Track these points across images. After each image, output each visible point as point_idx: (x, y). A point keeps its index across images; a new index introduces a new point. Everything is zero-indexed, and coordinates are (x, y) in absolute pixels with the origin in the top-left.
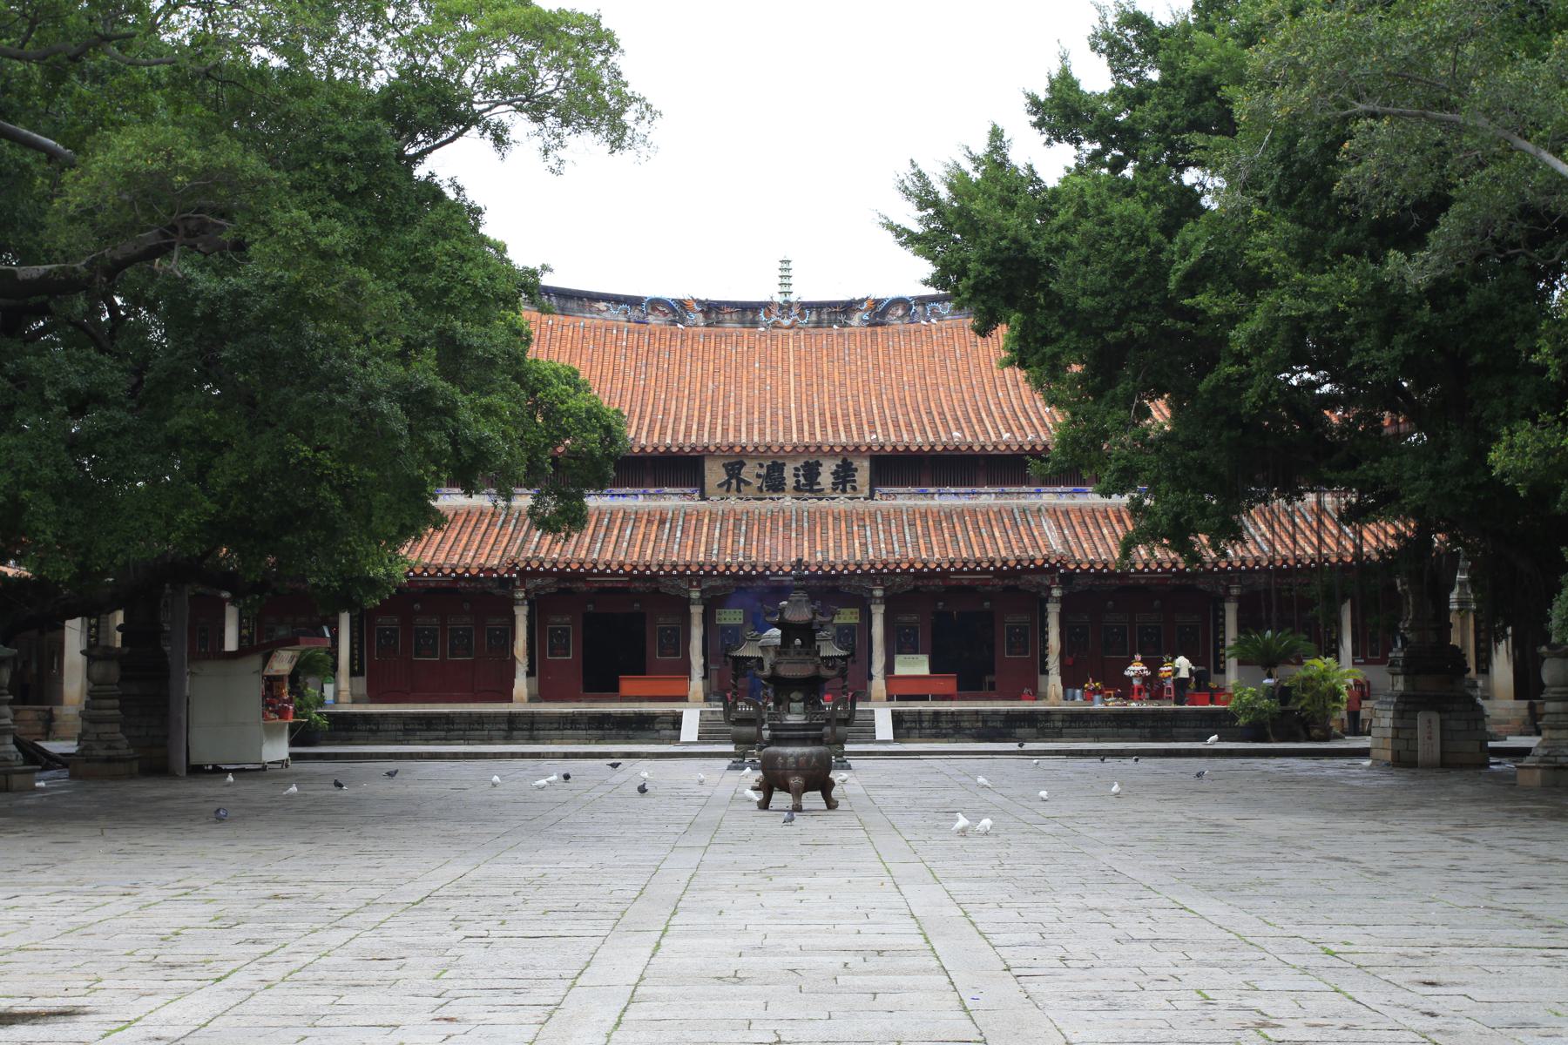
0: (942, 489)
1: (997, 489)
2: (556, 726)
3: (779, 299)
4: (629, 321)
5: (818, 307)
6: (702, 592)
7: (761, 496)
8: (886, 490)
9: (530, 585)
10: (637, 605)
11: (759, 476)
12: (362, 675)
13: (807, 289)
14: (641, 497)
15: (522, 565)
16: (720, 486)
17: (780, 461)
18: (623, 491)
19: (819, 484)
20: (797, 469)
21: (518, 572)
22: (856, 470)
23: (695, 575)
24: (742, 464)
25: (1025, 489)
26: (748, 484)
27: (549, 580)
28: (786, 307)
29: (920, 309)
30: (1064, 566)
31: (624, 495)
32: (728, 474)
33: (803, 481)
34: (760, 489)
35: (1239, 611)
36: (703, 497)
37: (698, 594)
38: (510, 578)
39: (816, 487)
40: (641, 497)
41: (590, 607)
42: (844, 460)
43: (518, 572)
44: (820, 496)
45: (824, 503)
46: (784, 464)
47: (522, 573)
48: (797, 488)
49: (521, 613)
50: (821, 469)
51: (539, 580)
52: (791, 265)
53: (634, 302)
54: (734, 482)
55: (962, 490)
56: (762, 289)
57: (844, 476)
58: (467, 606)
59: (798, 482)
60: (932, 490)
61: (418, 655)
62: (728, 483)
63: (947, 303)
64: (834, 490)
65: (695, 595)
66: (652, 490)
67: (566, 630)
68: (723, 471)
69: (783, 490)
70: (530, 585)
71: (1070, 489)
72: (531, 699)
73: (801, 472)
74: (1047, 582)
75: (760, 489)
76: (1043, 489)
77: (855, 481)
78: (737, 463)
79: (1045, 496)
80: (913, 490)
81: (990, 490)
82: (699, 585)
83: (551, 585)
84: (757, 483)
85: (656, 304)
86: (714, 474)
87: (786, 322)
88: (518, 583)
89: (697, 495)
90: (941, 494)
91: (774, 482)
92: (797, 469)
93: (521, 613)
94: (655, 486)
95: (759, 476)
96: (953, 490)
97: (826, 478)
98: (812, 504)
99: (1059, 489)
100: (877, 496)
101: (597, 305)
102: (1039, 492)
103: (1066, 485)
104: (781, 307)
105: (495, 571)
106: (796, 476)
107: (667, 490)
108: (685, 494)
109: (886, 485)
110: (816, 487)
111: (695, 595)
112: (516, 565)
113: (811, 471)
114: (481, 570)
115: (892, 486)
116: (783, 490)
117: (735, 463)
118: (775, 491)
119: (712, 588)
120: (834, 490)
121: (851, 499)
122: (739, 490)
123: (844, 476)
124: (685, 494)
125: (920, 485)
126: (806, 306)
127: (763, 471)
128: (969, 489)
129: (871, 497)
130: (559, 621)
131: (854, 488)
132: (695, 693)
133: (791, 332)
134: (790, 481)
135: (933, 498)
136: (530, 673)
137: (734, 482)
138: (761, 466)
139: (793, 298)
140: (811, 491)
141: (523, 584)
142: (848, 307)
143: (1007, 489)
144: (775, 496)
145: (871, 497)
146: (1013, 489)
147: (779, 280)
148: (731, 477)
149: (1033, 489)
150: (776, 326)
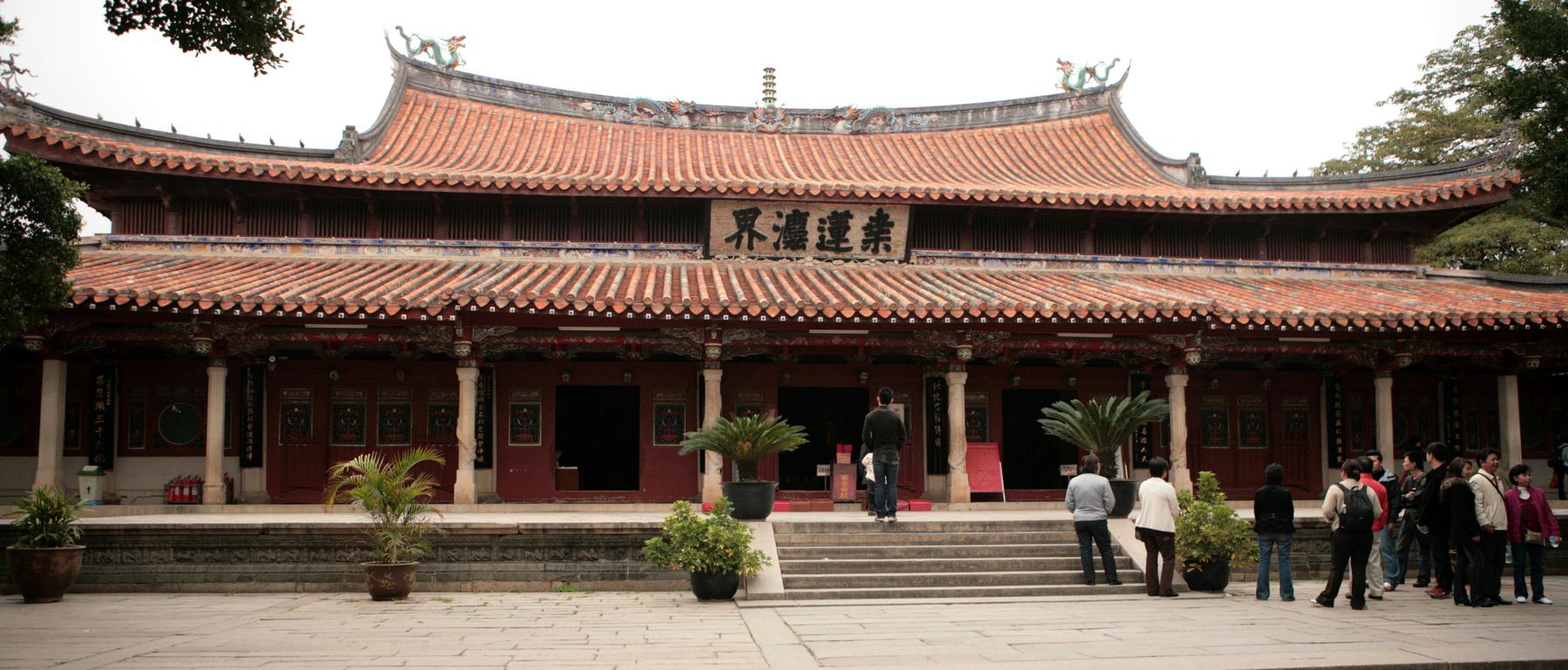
0: (988, 254)
1: (1050, 256)
2: (482, 553)
3: (763, 105)
4: (614, 122)
5: (803, 115)
6: (724, 349)
7: (778, 254)
8: (924, 252)
9: (478, 336)
10: (628, 375)
11: (776, 229)
12: (260, 465)
13: (789, 97)
14: (631, 253)
15: (463, 303)
16: (728, 240)
17: (802, 210)
18: (610, 245)
19: (847, 241)
20: (822, 221)
21: (458, 314)
22: (892, 224)
23: (716, 320)
24: (757, 213)
25: (1078, 256)
26: (762, 238)
27: (506, 330)
28: (770, 114)
29: (900, 120)
30: (1216, 319)
31: (610, 251)
32: (739, 226)
33: (828, 236)
34: (776, 246)
35: (1396, 393)
36: (707, 256)
37: (717, 351)
38: (447, 323)
39: (843, 245)
40: (631, 253)
41: (566, 378)
42: (880, 211)
43: (458, 314)
44: (847, 256)
45: (851, 265)
46: (807, 214)
47: (464, 314)
48: (821, 246)
49: (468, 378)
50: (851, 222)
51: (491, 330)
52: (775, 74)
53: (622, 104)
54: (746, 235)
55: (1011, 255)
56: (748, 96)
57: (877, 232)
58: (401, 376)
59: (822, 238)
60: (976, 254)
61: (337, 440)
62: (738, 237)
63: (925, 116)
64: (864, 249)
65: (713, 352)
66: (645, 246)
67: (535, 409)
68: (733, 221)
69: (804, 247)
70: (478, 336)
71: (1130, 258)
72: (482, 499)
73: (827, 226)
74: (1182, 345)
75: (776, 246)
76: (1100, 257)
77: (889, 239)
78: (750, 211)
79: (1101, 266)
80: (955, 253)
81: (1042, 256)
82: (719, 339)
83: (511, 342)
84: (773, 237)
85: (642, 105)
86: (722, 223)
87: (770, 127)
88: (460, 332)
89: (699, 252)
90: (985, 259)
91: (793, 236)
92: (822, 221)
93: (468, 378)
94: (648, 241)
95: (776, 229)
96: (1000, 255)
97: (855, 235)
98: (838, 267)
99: (1117, 258)
100: (913, 260)
101: (583, 105)
102: (1095, 261)
103: (1124, 254)
104: (766, 113)
105: (424, 311)
106: (821, 229)
107: (663, 245)
108: (685, 251)
109: (922, 247)
110: (843, 245)
111: (713, 352)
112: (455, 302)
113: (839, 224)
114: (403, 310)
115: (931, 248)
116: (804, 247)
117: (747, 206)
118: (793, 249)
119: (737, 345)
120: (864, 249)
121: (884, 261)
122: (750, 247)
123: (877, 232)
124: (685, 251)
125: (959, 249)
126: (790, 114)
127: (782, 223)
128: (1017, 255)
129: (907, 259)
130: (527, 397)
131: (888, 248)
132: (711, 490)
133: (776, 136)
134: (813, 237)
135: (976, 264)
136: (481, 464)
137: (746, 235)
138: (780, 215)
139: (777, 104)
140: (838, 250)
141: (468, 335)
142: (833, 115)
143: (1060, 256)
144: (793, 255)
145: (907, 259)
146: (1068, 257)
147: (764, 88)
148: (742, 228)
149: (1089, 257)
150: (761, 131)
